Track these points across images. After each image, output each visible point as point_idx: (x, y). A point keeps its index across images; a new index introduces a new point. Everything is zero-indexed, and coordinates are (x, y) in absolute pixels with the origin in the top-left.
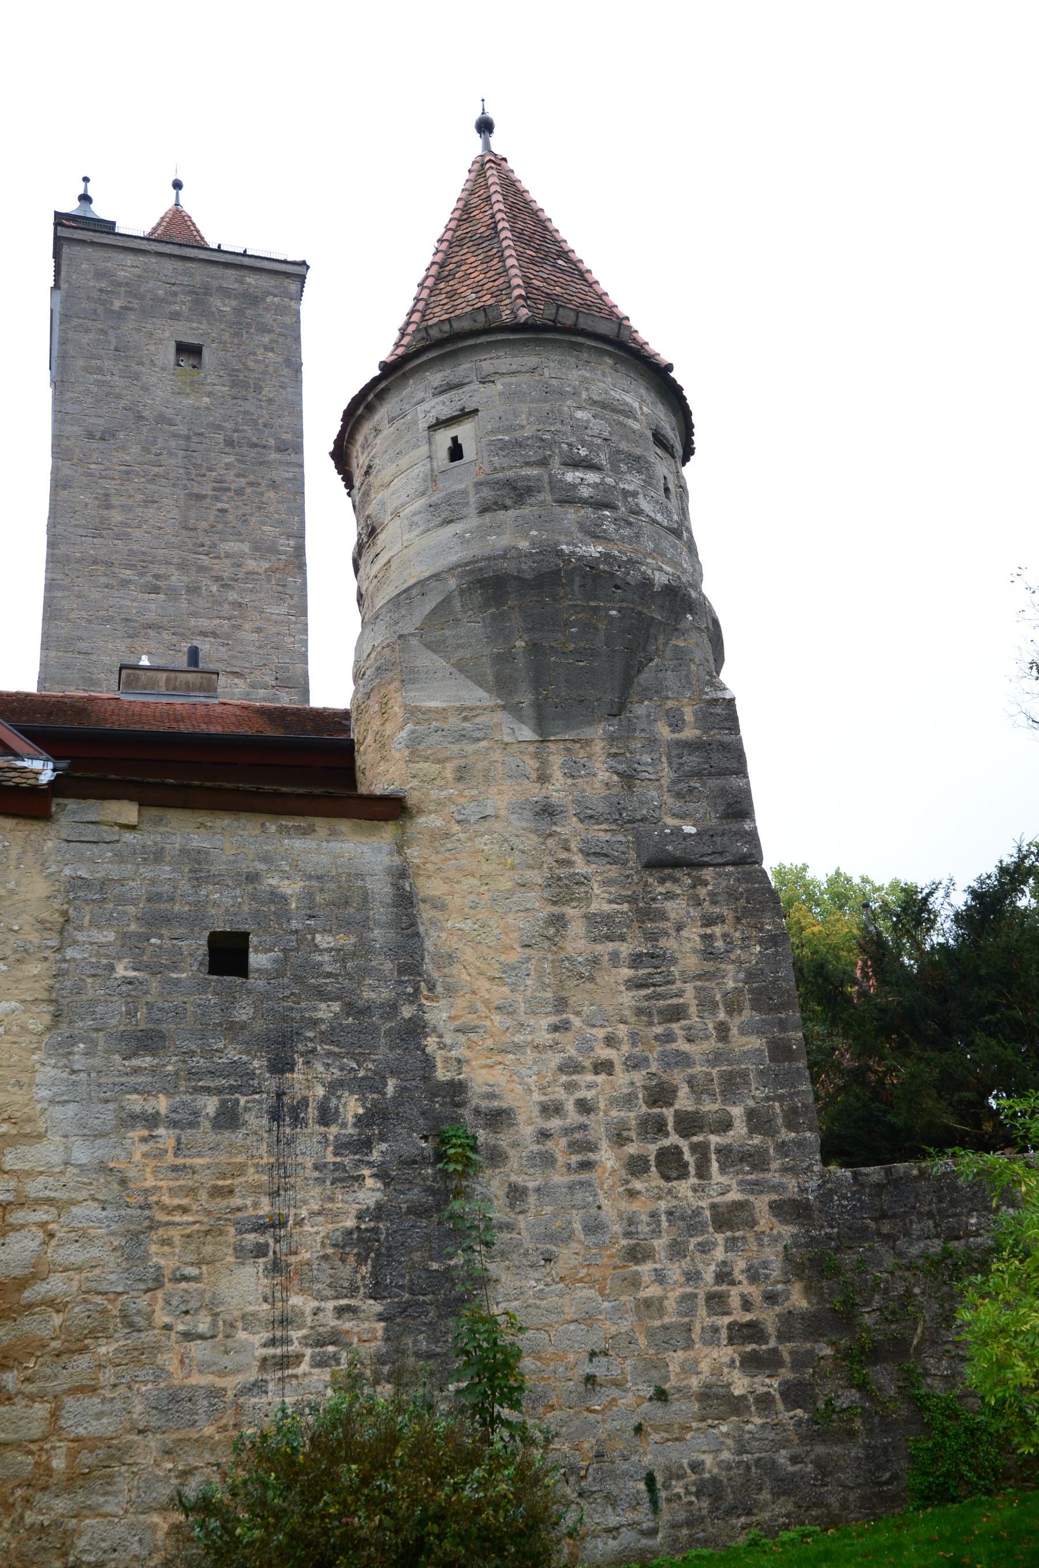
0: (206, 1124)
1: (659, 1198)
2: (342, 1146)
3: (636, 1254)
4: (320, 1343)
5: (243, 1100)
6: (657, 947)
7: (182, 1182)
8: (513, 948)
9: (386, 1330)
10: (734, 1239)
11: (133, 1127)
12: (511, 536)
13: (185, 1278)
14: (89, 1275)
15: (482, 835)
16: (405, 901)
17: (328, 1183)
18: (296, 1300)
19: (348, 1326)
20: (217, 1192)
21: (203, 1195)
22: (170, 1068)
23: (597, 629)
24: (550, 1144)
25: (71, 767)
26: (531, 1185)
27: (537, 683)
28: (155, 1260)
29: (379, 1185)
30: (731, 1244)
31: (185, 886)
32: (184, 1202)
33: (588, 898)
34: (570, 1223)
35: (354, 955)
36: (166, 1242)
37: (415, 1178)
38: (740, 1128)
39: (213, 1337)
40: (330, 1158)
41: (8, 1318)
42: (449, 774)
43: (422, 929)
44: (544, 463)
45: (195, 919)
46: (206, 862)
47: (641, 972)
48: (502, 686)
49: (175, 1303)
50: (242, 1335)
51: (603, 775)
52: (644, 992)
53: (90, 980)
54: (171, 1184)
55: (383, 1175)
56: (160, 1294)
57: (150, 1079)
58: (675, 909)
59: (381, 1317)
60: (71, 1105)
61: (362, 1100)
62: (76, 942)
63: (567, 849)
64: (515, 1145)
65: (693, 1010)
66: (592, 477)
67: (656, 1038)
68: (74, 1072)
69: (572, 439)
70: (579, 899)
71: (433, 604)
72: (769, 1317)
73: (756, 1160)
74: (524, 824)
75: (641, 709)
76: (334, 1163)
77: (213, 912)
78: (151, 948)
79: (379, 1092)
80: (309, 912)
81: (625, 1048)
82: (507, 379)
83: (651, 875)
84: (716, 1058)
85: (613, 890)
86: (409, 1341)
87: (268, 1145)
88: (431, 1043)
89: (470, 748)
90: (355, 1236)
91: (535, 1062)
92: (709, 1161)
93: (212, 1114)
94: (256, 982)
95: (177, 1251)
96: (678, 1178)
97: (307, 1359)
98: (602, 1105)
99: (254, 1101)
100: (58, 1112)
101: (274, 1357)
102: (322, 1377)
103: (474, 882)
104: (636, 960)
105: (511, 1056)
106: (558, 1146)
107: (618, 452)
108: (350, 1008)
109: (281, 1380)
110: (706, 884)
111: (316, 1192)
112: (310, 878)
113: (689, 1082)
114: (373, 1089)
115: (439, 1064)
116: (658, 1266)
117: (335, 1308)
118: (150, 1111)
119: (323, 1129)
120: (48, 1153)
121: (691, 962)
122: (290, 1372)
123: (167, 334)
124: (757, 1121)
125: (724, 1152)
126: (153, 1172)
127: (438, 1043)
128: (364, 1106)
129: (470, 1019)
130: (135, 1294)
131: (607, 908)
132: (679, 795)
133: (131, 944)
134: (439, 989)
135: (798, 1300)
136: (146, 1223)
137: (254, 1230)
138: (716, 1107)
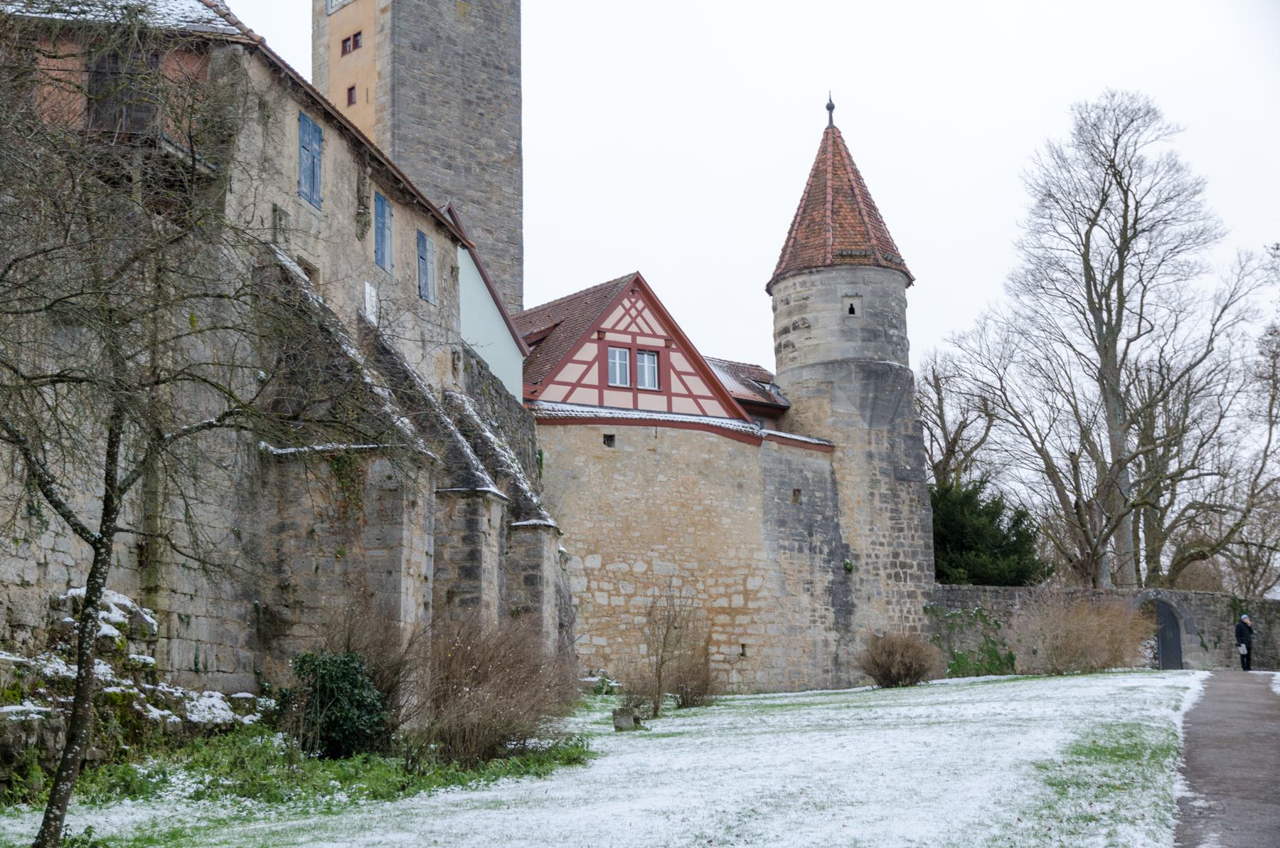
3: (888, 603)
16: (834, 482)
38: (915, 568)
72: (919, 625)
73: (919, 579)
84: (911, 546)
106: (871, 567)
108: (825, 518)
124: (920, 567)
125: (911, 575)
133: (778, 490)
135: (926, 622)
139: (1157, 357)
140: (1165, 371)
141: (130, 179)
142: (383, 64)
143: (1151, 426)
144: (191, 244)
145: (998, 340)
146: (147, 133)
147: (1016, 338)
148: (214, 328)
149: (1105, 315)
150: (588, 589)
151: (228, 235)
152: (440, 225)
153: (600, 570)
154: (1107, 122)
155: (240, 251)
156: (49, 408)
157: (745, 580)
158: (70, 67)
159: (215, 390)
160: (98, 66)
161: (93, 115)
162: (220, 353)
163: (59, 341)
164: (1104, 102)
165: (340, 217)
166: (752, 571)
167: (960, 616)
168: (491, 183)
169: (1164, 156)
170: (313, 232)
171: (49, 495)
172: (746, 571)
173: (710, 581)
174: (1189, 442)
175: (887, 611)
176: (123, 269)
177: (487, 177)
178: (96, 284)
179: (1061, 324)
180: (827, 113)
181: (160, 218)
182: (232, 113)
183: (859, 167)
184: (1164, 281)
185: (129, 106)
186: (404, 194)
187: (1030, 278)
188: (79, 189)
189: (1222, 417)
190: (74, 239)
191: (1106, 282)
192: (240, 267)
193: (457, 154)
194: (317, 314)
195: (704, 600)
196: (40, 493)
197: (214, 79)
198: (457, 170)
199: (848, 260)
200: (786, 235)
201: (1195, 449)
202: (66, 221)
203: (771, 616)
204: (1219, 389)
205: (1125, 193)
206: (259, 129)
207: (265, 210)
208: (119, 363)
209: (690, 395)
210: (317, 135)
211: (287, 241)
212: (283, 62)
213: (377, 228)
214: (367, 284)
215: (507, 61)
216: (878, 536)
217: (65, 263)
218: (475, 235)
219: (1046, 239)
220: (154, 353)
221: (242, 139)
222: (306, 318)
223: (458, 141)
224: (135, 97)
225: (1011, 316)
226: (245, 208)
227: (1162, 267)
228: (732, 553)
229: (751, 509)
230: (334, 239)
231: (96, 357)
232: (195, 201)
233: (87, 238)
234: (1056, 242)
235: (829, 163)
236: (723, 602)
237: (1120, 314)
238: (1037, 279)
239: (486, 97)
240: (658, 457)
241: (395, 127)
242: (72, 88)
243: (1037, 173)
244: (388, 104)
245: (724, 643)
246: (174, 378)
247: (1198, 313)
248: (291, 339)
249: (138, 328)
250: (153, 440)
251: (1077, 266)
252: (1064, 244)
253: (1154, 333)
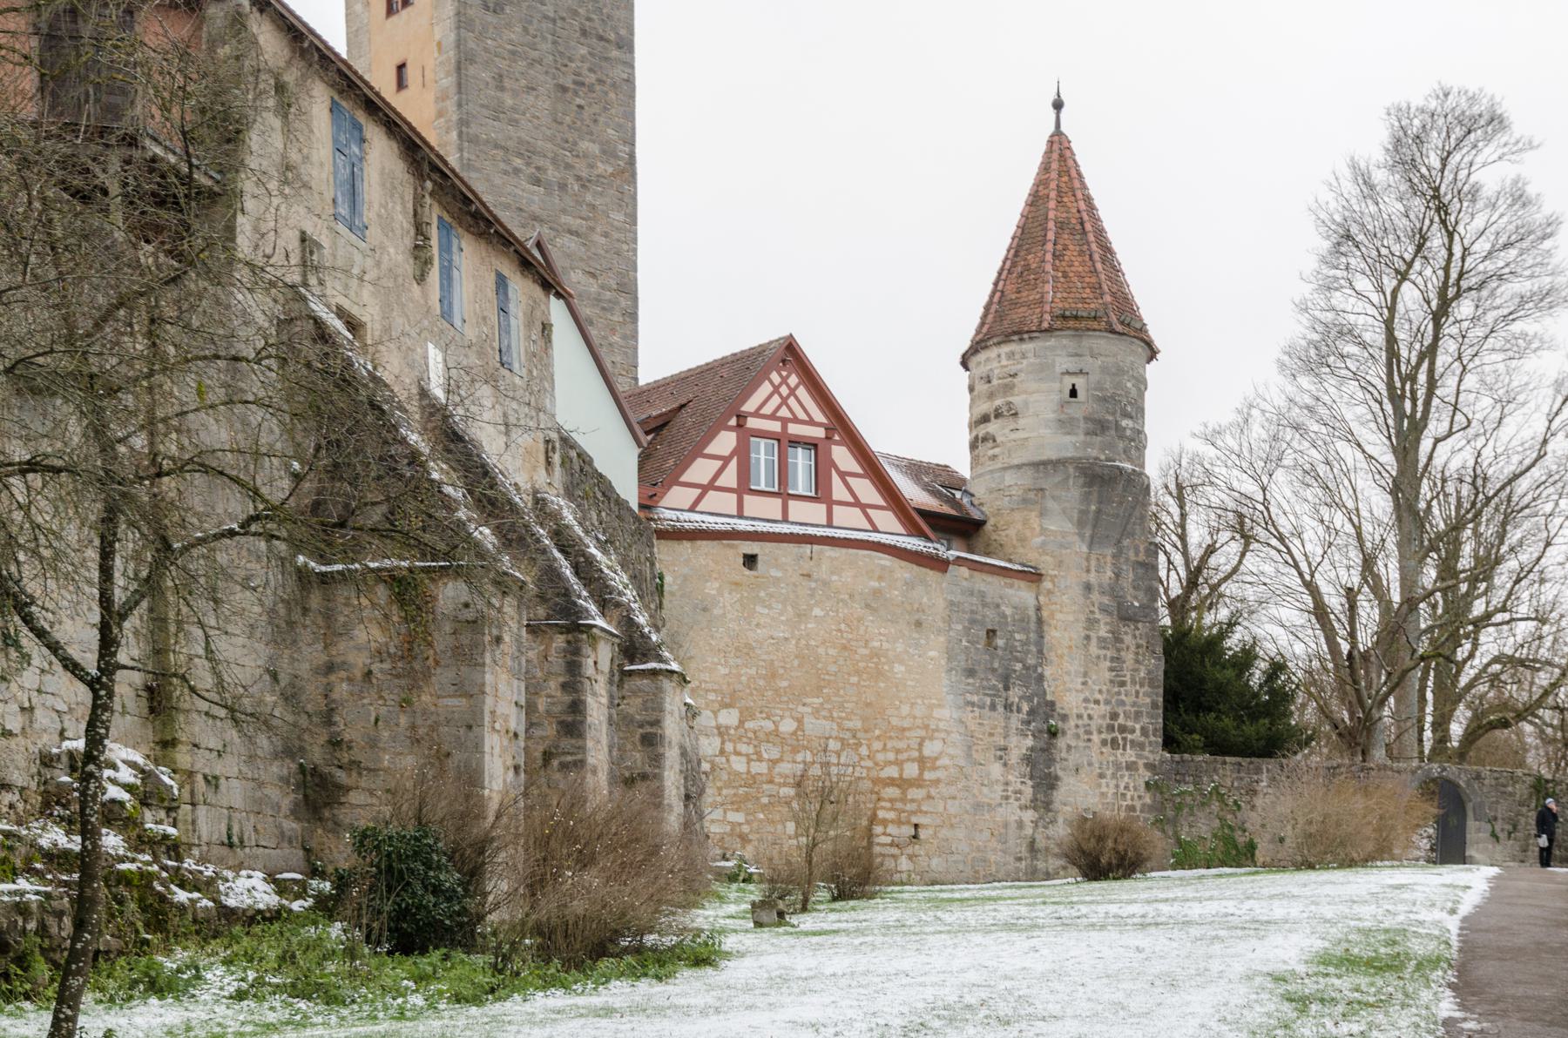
3: (1101, 776)
16: (1040, 621)
27: (1095, 526)
38: (1138, 732)
58: (1128, 639)
73: (1141, 746)
84: (1134, 704)
104: (1112, 659)
106: (1081, 731)
108: (1026, 668)
124: (1144, 732)
125: (1132, 742)
133: (967, 630)
135: (1148, 800)
139: (1471, 463)
140: (1479, 482)
141: (105, 192)
142: (445, 31)
143: (1455, 555)
144: (192, 286)
145: (1264, 436)
146: (124, 126)
147: (1289, 434)
148: (229, 402)
149: (1408, 405)
150: (722, 752)
151: (242, 273)
152: (525, 264)
153: (737, 728)
154: (1435, 134)
155: (259, 296)
156: (20, 507)
157: (921, 745)
158: (12, 26)
159: (235, 487)
160: (50, 26)
161: (48, 98)
162: (240, 437)
163: (26, 417)
164: (1433, 104)
165: (392, 250)
166: (930, 733)
167: (1191, 794)
168: (593, 207)
169: (1508, 182)
170: (355, 271)
171: (28, 620)
172: (923, 733)
173: (877, 745)
174: (1502, 578)
175: (1100, 786)
176: (104, 319)
177: (589, 198)
178: (70, 339)
179: (1348, 416)
180: (1052, 113)
181: (149, 248)
182: (240, 98)
183: (1093, 192)
184: (1491, 360)
185: (97, 86)
186: (479, 222)
187: (1313, 352)
188: (37, 205)
189: (1548, 544)
190: (35, 276)
191: (1414, 361)
192: (261, 320)
193: (547, 164)
194: (365, 386)
195: (869, 769)
196: (16, 618)
197: (212, 49)
198: (548, 186)
199: (1071, 323)
200: (991, 287)
201: (1509, 586)
202: (23, 250)
203: (952, 790)
204: (1548, 508)
205: (1451, 235)
206: (277, 123)
207: (290, 239)
208: (107, 448)
209: (857, 503)
210: (356, 133)
211: (321, 283)
212: (305, 25)
213: (442, 267)
214: (431, 346)
215: (614, 29)
217: (26, 309)
218: (574, 279)
219: (1337, 299)
220: (151, 434)
221: (254, 137)
222: (351, 391)
223: (549, 146)
224: (104, 74)
225: (1281, 402)
226: (263, 235)
227: (1490, 340)
228: (905, 710)
229: (932, 654)
230: (384, 282)
231: (76, 439)
232: (196, 226)
233: (53, 274)
234: (1352, 303)
235: (1053, 185)
236: (892, 772)
237: (1427, 403)
238: (1320, 355)
239: (587, 81)
240: (813, 585)
241: (463, 123)
242: (17, 58)
243: (1333, 205)
244: (453, 90)
245: (892, 821)
246: (181, 469)
247: (1532, 405)
248: (332, 418)
249: (129, 400)
250: (158, 550)
251: (1376, 337)
252: (1361, 306)
253: (1471, 431)
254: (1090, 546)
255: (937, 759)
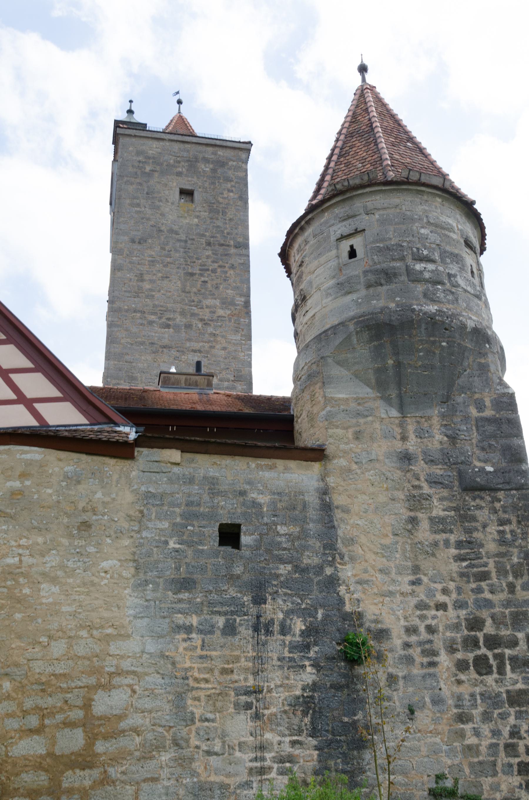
0: (218, 633)
1: (476, 686)
2: (293, 648)
3: (463, 718)
4: (281, 761)
5: (238, 620)
6: (471, 537)
7: (205, 665)
8: (387, 535)
9: (319, 755)
10: (521, 712)
11: (179, 632)
12: (384, 301)
13: (207, 720)
14: (155, 715)
15: (370, 471)
16: (327, 507)
17: (286, 668)
18: (268, 736)
19: (297, 752)
20: (225, 671)
21: (217, 673)
22: (198, 600)
23: (434, 353)
24: (411, 651)
25: (145, 431)
26: (400, 674)
28: (191, 708)
29: (314, 671)
30: (519, 715)
31: (206, 497)
32: (206, 676)
33: (431, 509)
34: (424, 698)
35: (299, 538)
36: (198, 699)
37: (334, 667)
39: (223, 754)
40: (287, 654)
41: (112, 737)
42: (350, 435)
43: (336, 523)
44: (402, 259)
45: (211, 516)
46: (218, 484)
47: (462, 552)
48: (380, 385)
49: (201, 734)
50: (238, 754)
51: (438, 437)
52: (464, 564)
53: (155, 549)
54: (200, 666)
55: (316, 665)
56: (193, 728)
57: (188, 606)
58: (483, 515)
59: (317, 748)
60: (146, 619)
61: (304, 621)
62: (148, 528)
63: (418, 479)
64: (391, 650)
65: (494, 575)
66: (431, 267)
67: (472, 590)
68: (147, 600)
69: (419, 246)
70: (426, 509)
71: (341, 340)
74: (393, 465)
75: (460, 399)
76: (289, 657)
77: (222, 512)
78: (188, 532)
79: (314, 617)
80: (274, 513)
81: (454, 596)
82: (381, 212)
83: (467, 495)
84: (508, 604)
85: (445, 503)
86: (332, 763)
87: (253, 646)
88: (342, 589)
89: (362, 421)
90: (301, 700)
91: (401, 602)
92: (504, 664)
93: (221, 627)
94: (245, 552)
95: (203, 704)
96: (486, 674)
97: (275, 770)
98: (441, 629)
99: (244, 620)
100: (139, 623)
101: (256, 768)
102: (284, 781)
103: (364, 497)
104: (459, 545)
105: (387, 598)
106: (416, 652)
107: (445, 252)
108: (297, 568)
109: (261, 781)
110: (499, 500)
111: (279, 673)
112: (274, 494)
113: (492, 617)
114: (310, 616)
115: (347, 602)
116: (476, 726)
117: (290, 741)
118: (188, 624)
119: (282, 637)
120: (132, 646)
121: (492, 547)
122: (265, 777)
123: (175, 184)
125: (513, 659)
126: (189, 659)
127: (346, 590)
128: (305, 625)
129: (365, 577)
130: (180, 727)
131: (442, 513)
132: (483, 449)
133: (178, 530)
134: (346, 558)
136: (186, 688)
137: (245, 694)
138: (508, 633)
216: (431, 593)
229: (105, 564)
254: (401, 408)
255: (120, 718)
